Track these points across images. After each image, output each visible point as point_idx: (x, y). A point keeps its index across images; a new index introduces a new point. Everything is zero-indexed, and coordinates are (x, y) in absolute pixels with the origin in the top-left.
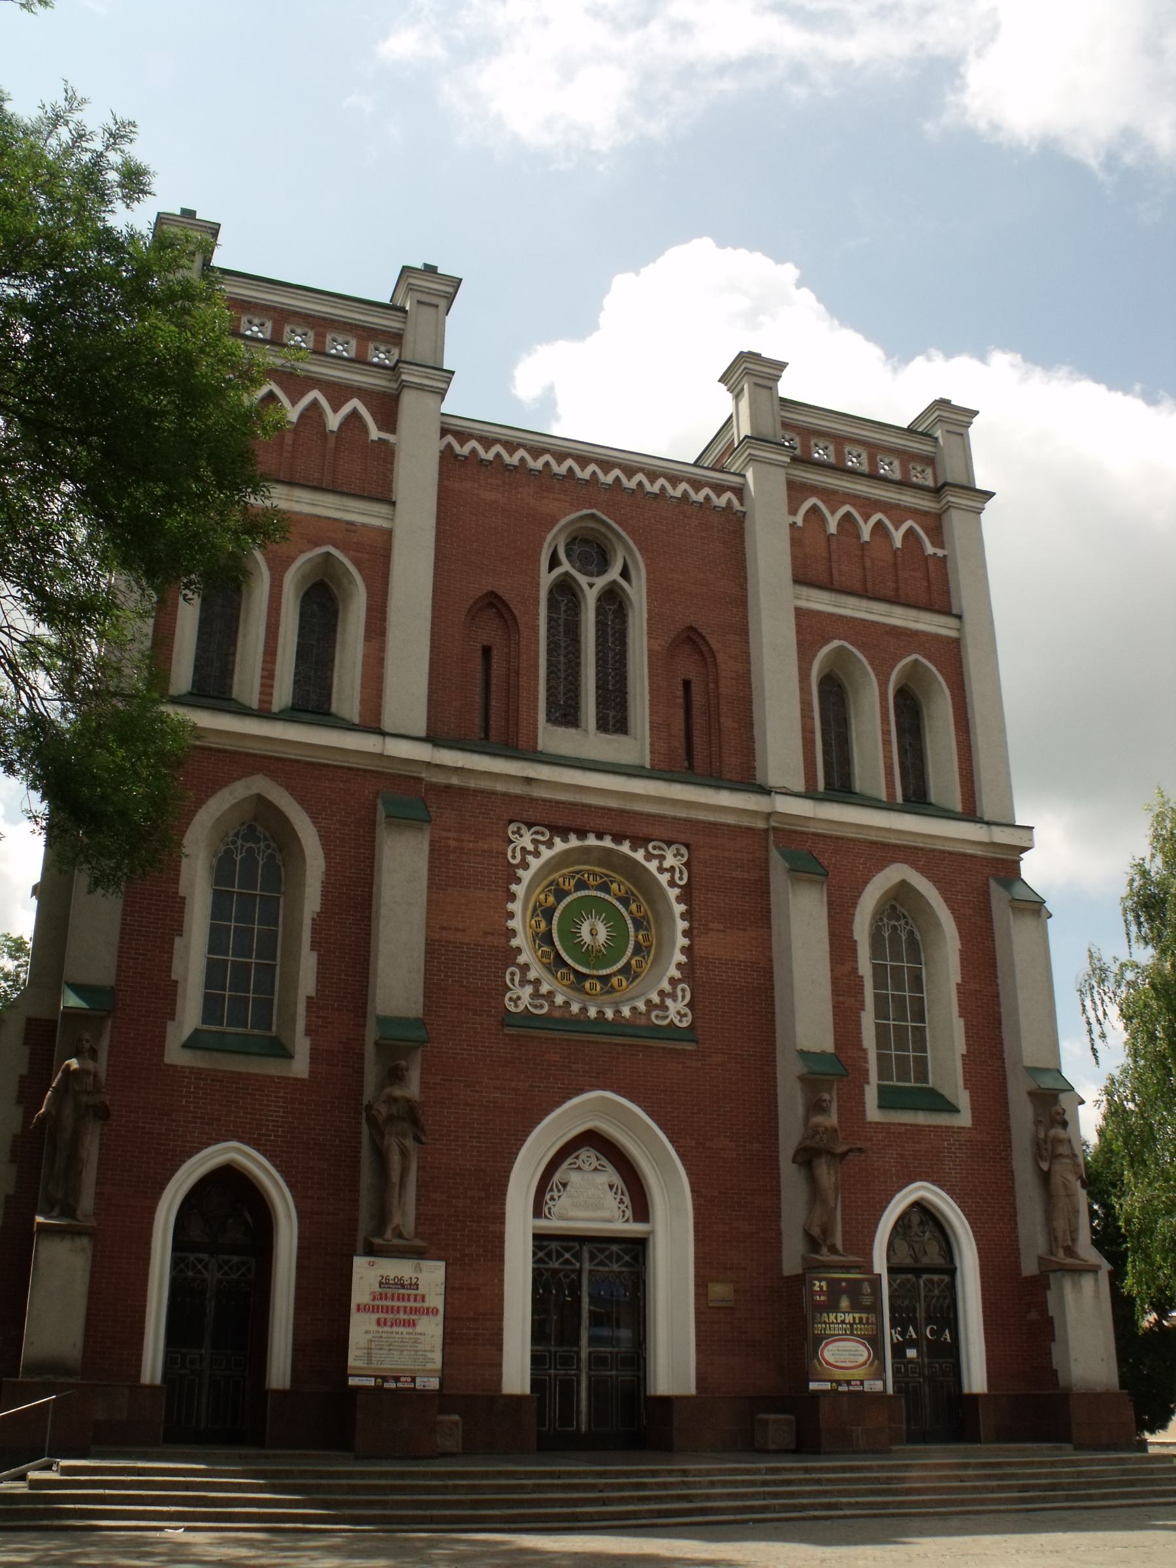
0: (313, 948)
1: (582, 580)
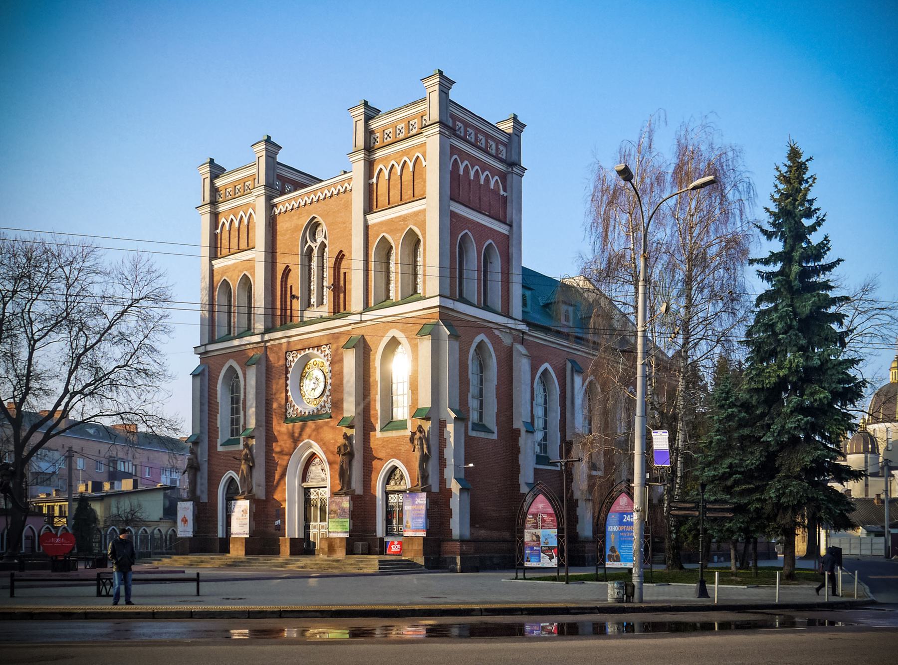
1: (313, 245)
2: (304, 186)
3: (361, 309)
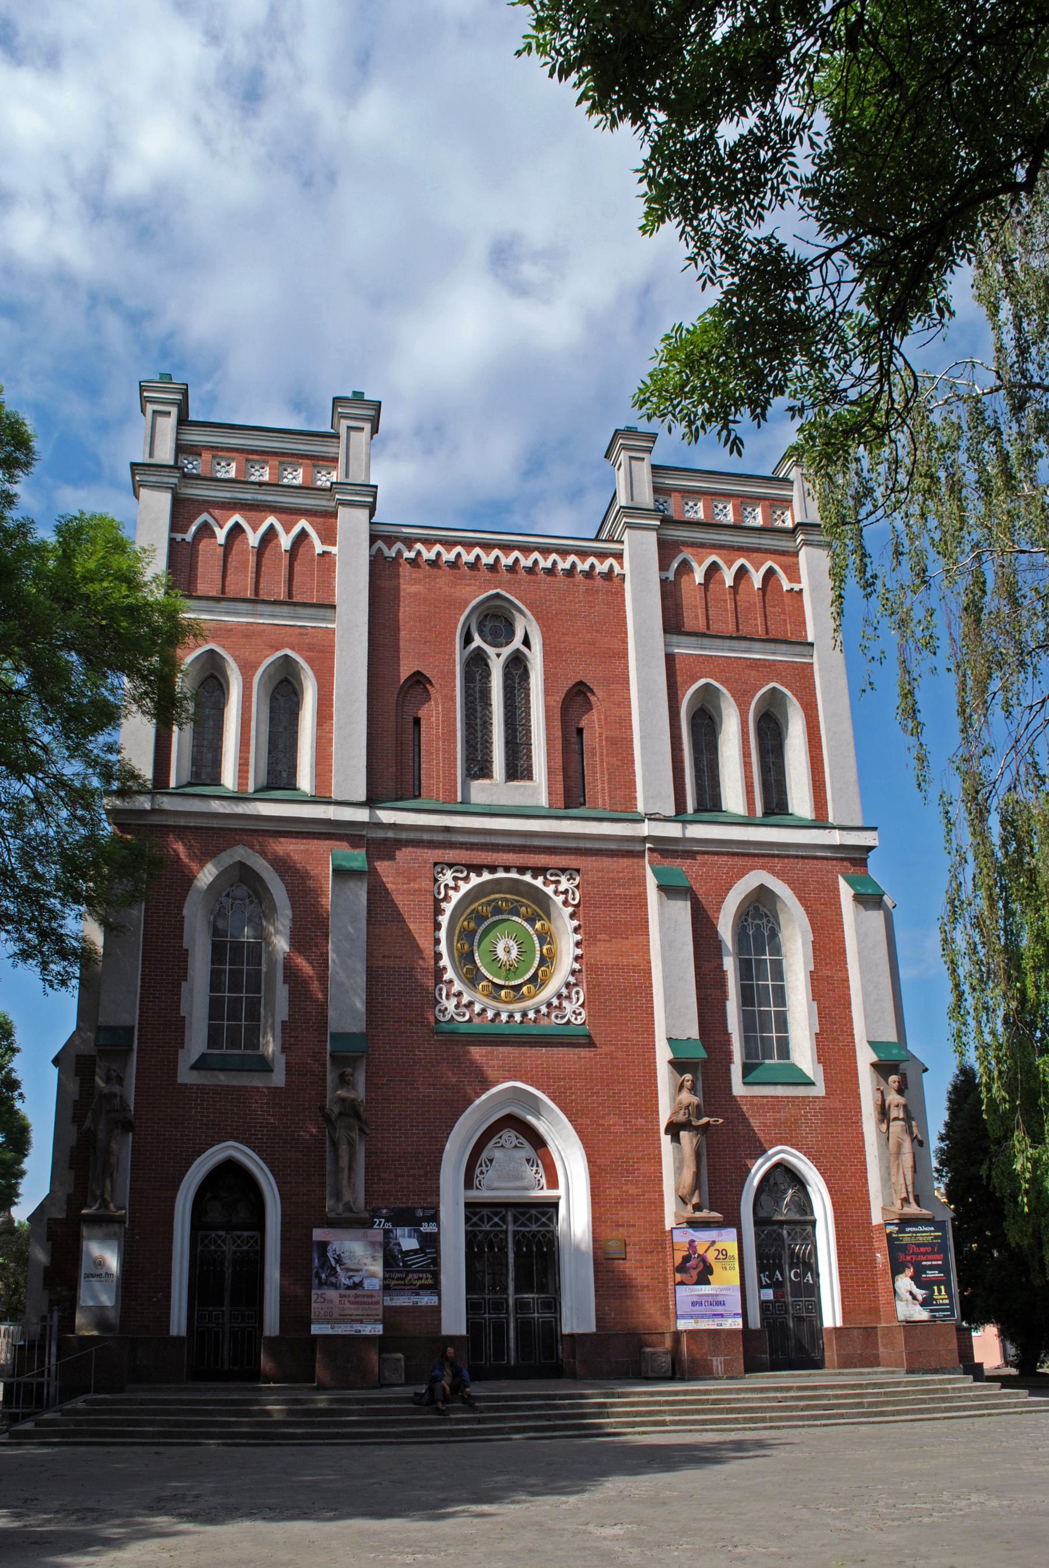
0: (285, 982)
1: (491, 651)
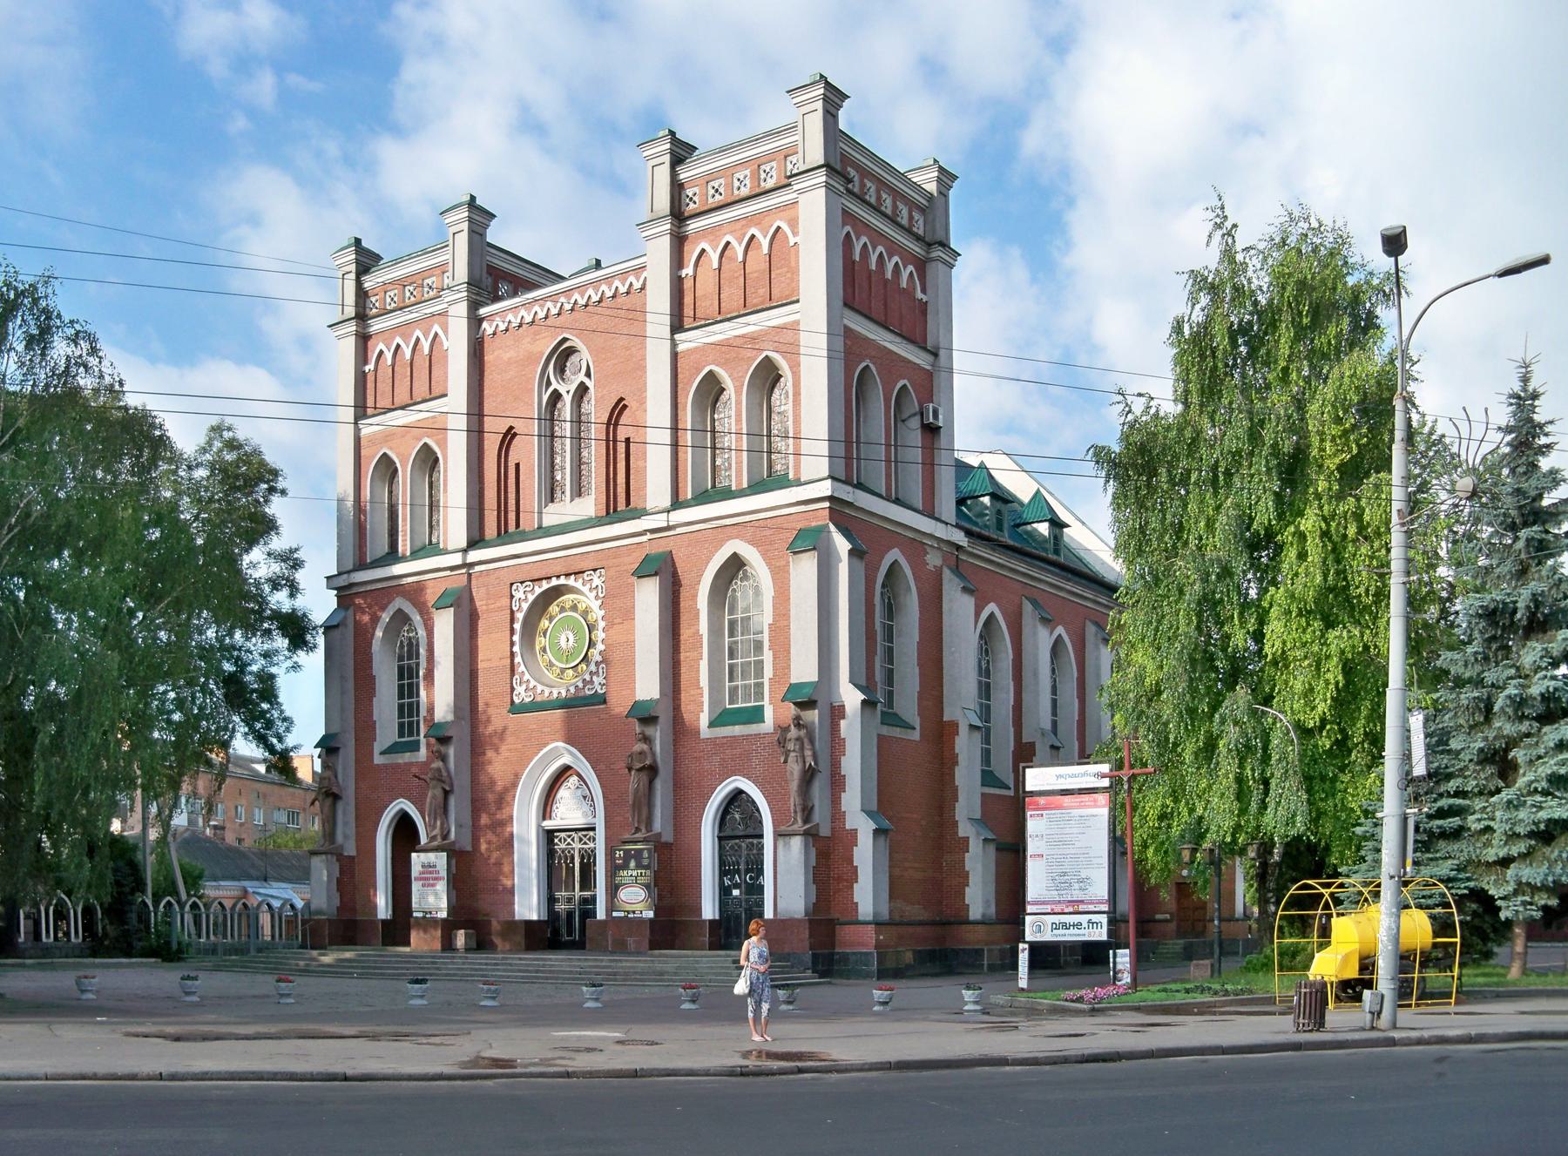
2: (531, 286)
3: (667, 503)
